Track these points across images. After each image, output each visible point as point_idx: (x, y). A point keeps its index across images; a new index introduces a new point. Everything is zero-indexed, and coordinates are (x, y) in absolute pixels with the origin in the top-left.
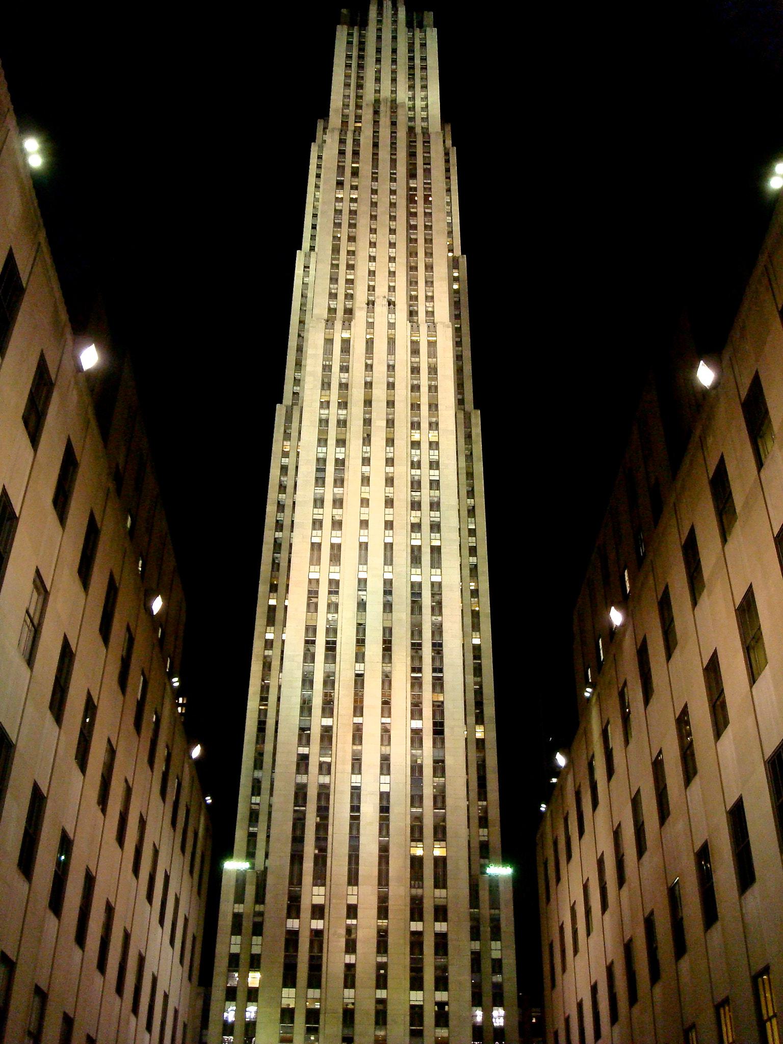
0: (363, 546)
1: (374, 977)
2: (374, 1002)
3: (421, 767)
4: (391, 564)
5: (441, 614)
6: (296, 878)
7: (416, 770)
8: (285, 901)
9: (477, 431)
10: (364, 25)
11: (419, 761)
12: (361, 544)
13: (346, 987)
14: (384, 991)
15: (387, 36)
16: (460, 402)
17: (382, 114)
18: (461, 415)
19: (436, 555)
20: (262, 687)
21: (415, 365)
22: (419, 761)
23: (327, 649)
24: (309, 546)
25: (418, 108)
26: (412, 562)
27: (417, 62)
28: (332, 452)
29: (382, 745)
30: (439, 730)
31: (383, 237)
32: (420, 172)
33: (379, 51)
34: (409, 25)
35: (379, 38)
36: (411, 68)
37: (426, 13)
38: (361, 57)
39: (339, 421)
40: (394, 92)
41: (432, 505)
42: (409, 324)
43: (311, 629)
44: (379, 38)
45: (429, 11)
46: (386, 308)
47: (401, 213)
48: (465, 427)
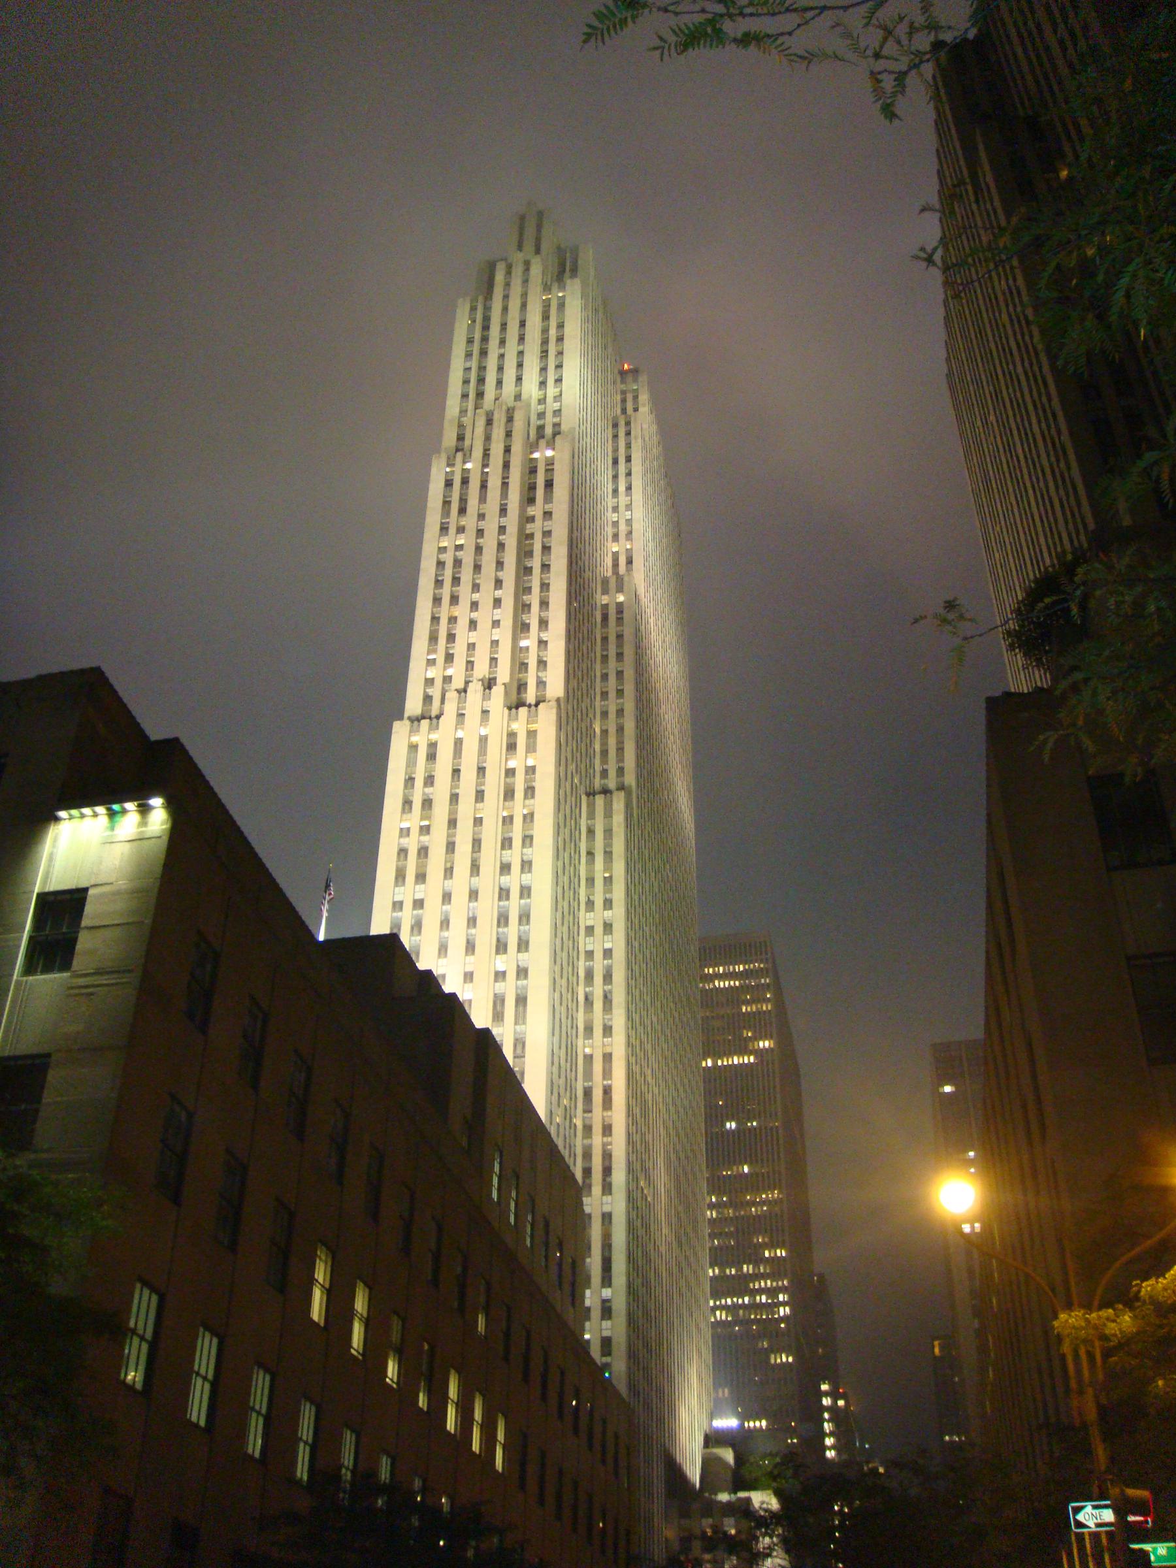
15: (514, 304)
17: (495, 424)
19: (521, 1009)
25: (550, 399)
27: (553, 332)
31: (485, 597)
33: (504, 326)
35: (505, 309)
36: (545, 342)
38: (485, 339)
42: (506, 711)
44: (505, 309)
47: (510, 558)
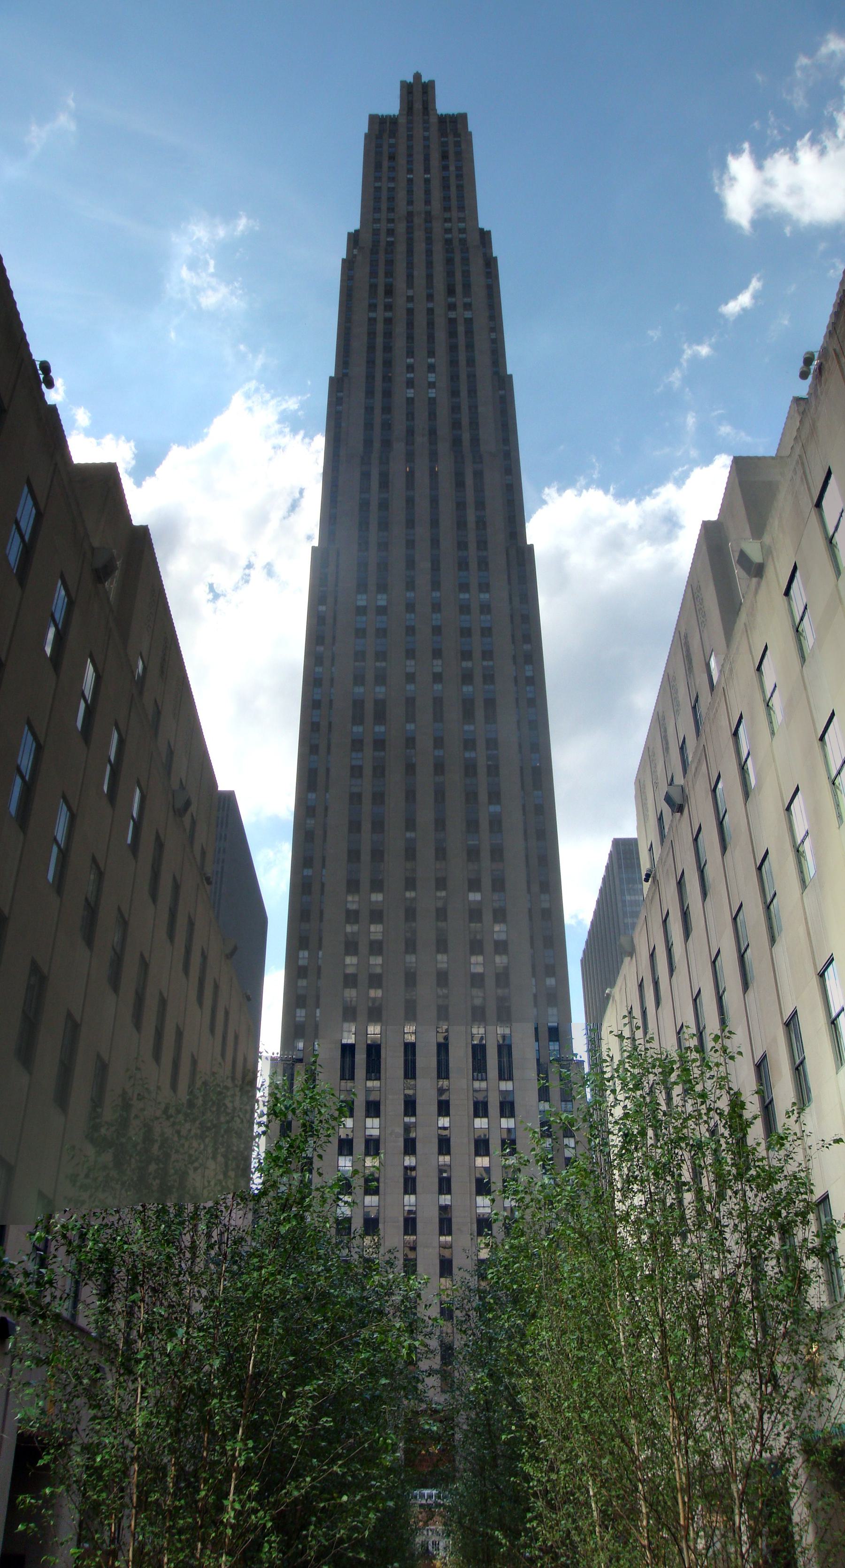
1: (436, 1180)
2: (437, 1208)
13: (406, 1192)
14: (448, 1197)
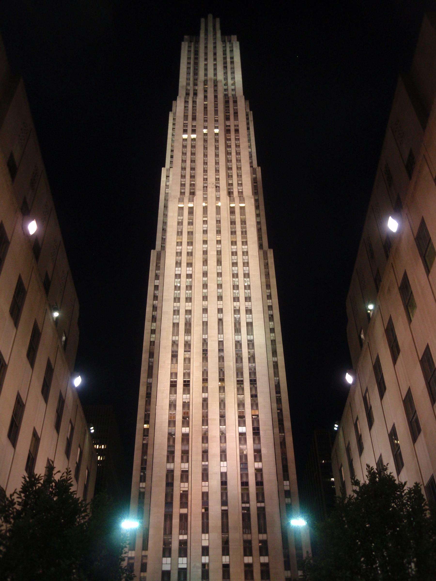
0: (205, 323)
3: (246, 456)
4: (223, 333)
5: (254, 362)
6: (168, 531)
7: (243, 458)
8: (161, 546)
9: (271, 261)
10: (197, 42)
11: (245, 453)
12: (203, 322)
16: (261, 246)
18: (262, 252)
20: (145, 415)
21: (233, 220)
22: (245, 453)
23: (184, 385)
24: (172, 325)
26: (235, 332)
27: (228, 60)
28: (184, 270)
29: (221, 442)
30: (256, 431)
32: (232, 117)
34: (224, 41)
35: (206, 47)
36: (225, 63)
37: (232, 36)
39: (188, 253)
40: (215, 75)
41: (246, 298)
42: (228, 198)
43: (174, 374)
44: (206, 47)
45: (234, 34)
46: (214, 189)
48: (264, 259)
